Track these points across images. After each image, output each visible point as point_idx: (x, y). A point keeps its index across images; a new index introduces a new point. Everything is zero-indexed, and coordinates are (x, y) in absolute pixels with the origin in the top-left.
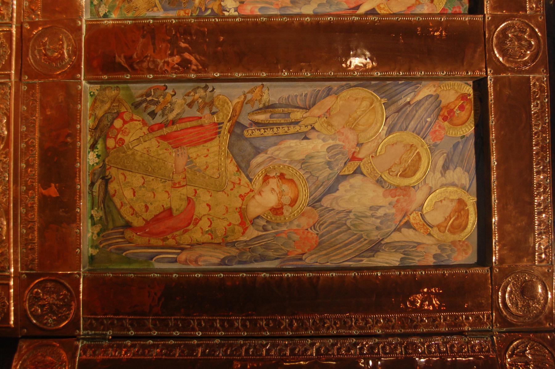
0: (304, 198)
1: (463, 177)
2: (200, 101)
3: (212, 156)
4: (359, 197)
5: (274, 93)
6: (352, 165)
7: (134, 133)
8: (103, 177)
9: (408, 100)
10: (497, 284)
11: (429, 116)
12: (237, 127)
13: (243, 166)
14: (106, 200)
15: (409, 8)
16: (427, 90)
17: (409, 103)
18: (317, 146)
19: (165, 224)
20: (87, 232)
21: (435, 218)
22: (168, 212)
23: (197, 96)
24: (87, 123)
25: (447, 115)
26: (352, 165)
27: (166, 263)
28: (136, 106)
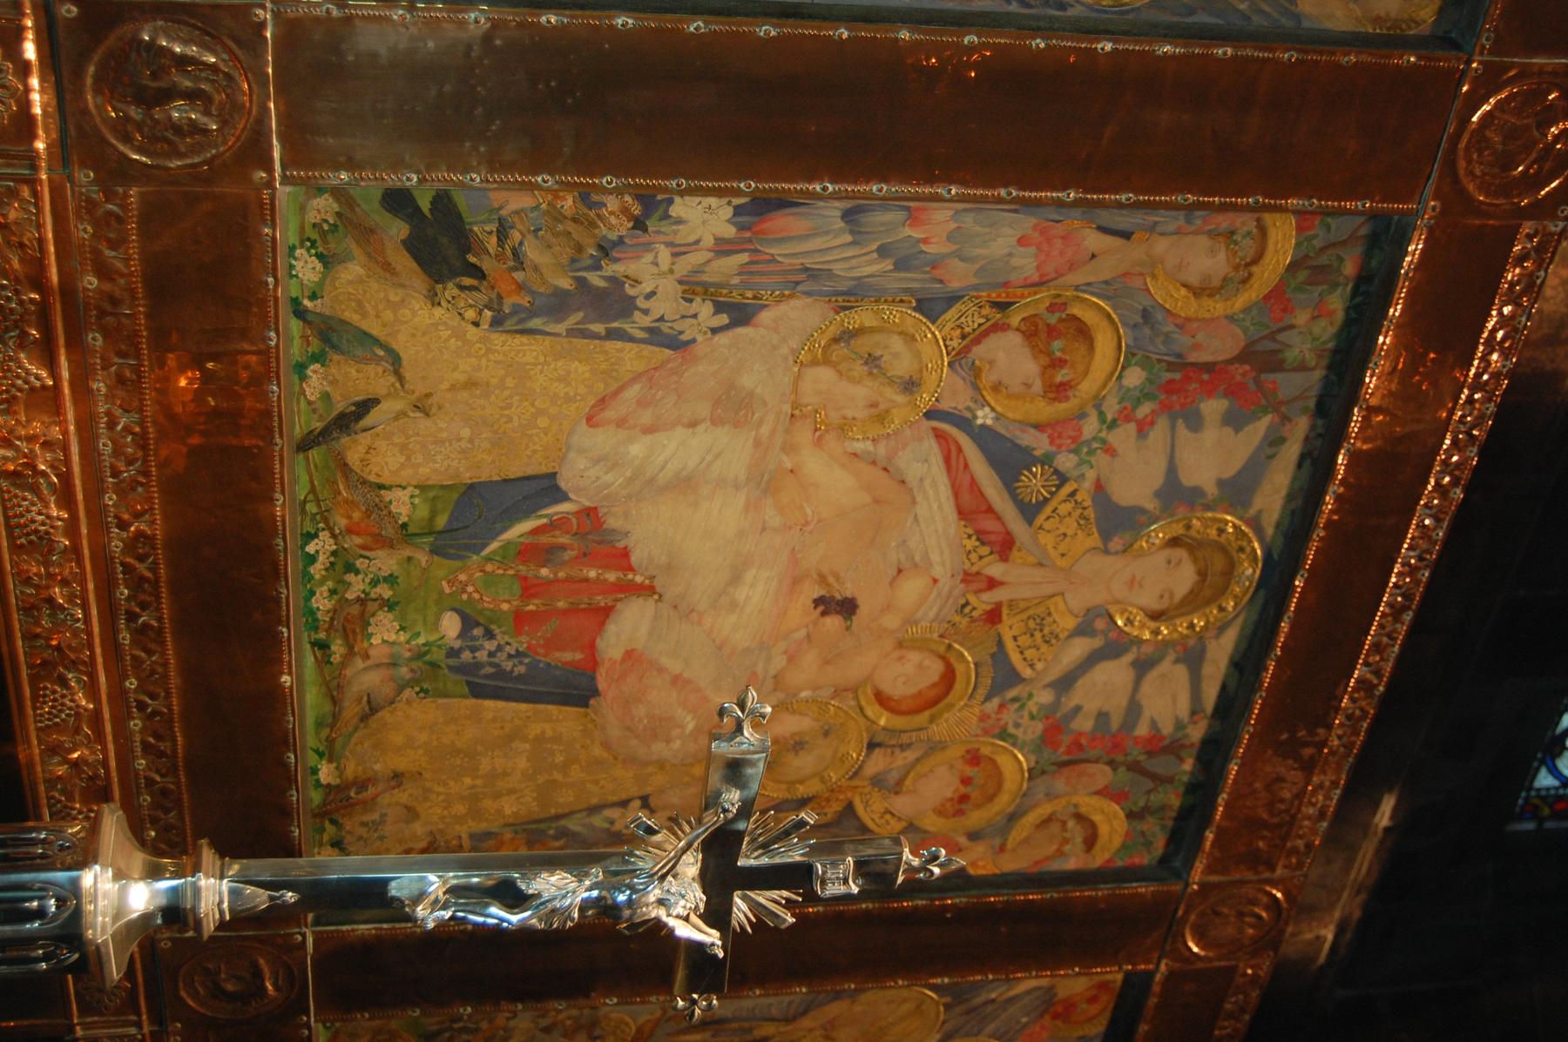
2: (569, 1022)
9: (993, 995)
11: (1027, 1014)
15: (1037, 863)
17: (993, 1001)
23: (561, 1017)
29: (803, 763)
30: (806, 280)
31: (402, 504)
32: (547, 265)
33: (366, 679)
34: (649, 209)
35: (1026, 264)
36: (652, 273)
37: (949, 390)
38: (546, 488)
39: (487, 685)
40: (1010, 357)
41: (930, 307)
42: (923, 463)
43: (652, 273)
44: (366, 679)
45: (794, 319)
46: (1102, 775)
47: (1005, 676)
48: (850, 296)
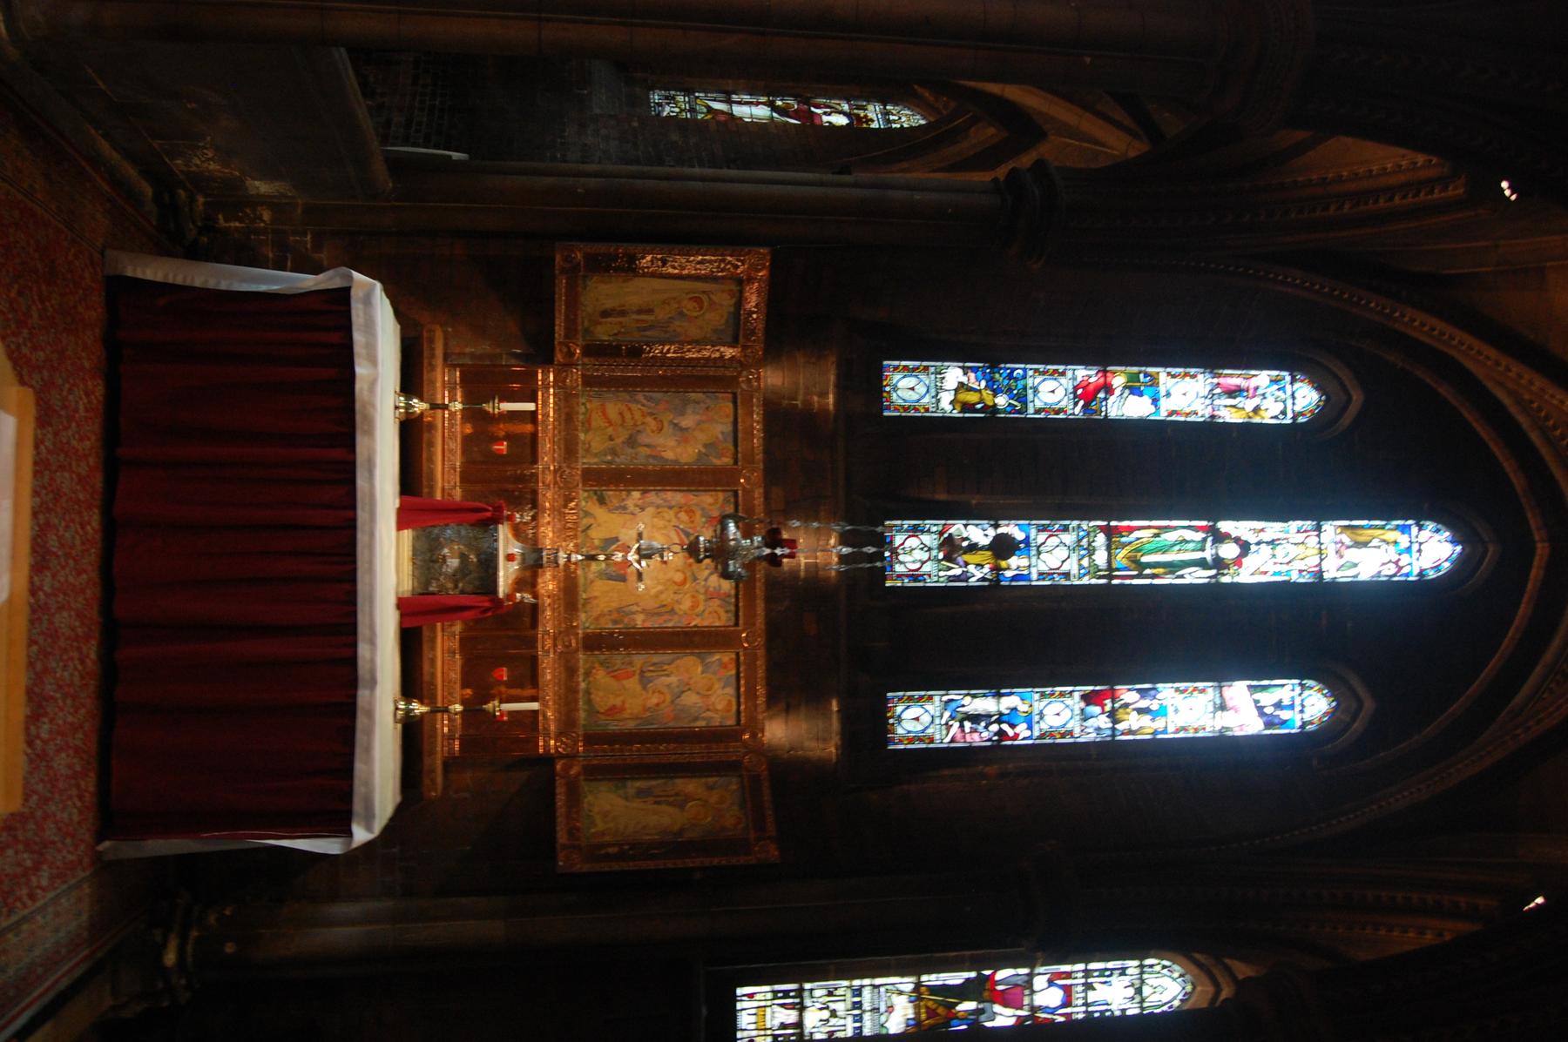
0: (669, 698)
1: (730, 691)
3: (632, 684)
4: (690, 699)
5: (656, 659)
6: (686, 687)
7: (600, 675)
8: (588, 692)
10: (743, 732)
12: (642, 672)
13: (644, 688)
14: (589, 702)
16: (717, 657)
18: (673, 679)
19: (613, 711)
20: (582, 714)
21: (719, 707)
22: (613, 707)
24: (581, 671)
25: (724, 666)
26: (686, 687)
27: (614, 727)
28: (601, 664)
29: (663, 597)
30: (652, 504)
31: (596, 542)
32: (616, 502)
33: (591, 576)
34: (629, 492)
35: (683, 501)
36: (630, 503)
37: (674, 522)
38: (616, 539)
39: (610, 578)
40: (683, 516)
41: (670, 508)
42: (673, 535)
43: (630, 503)
44: (591, 576)
45: (650, 510)
46: (717, 602)
47: (695, 579)
48: (658, 507)
